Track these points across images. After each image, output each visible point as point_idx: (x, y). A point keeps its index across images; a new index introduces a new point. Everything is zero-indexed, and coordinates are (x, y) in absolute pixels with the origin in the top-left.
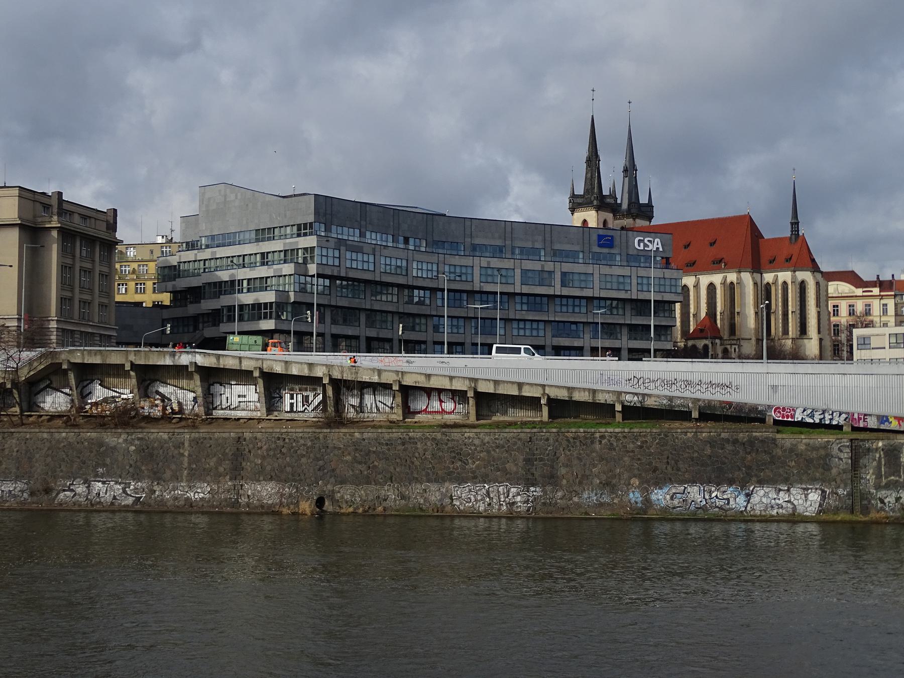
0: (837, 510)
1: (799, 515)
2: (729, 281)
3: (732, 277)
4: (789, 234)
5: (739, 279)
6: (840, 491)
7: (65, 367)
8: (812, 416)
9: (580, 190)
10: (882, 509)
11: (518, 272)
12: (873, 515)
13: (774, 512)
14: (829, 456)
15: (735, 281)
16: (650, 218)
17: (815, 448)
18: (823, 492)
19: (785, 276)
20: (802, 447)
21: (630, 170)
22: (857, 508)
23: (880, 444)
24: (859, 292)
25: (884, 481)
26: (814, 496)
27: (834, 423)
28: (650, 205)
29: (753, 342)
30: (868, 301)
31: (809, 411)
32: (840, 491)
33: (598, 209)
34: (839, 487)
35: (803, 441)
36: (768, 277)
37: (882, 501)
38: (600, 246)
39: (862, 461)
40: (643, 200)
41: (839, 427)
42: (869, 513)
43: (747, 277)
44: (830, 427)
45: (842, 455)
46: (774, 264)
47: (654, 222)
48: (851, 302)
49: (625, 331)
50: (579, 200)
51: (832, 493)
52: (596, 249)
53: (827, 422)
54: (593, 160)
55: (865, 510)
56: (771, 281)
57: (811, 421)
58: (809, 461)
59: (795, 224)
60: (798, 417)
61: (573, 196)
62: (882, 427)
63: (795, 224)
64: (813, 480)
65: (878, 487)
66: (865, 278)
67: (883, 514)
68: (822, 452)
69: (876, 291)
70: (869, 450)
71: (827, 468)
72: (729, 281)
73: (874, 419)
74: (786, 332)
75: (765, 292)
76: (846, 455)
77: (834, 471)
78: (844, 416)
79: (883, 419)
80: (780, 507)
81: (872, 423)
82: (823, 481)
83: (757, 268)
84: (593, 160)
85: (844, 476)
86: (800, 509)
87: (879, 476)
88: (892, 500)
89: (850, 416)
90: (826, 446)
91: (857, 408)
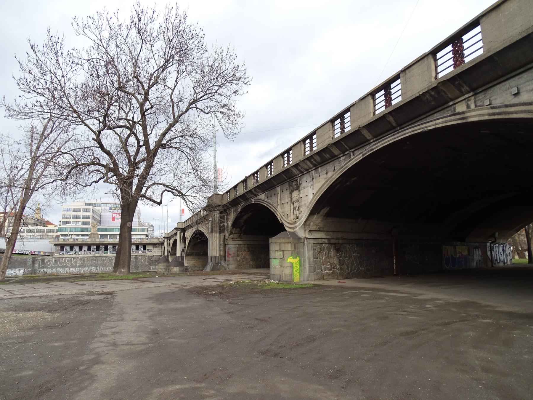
0: (28, 274)
1: (18, 276)
6: (29, 269)
8: (21, 252)
10: (39, 273)
12: (37, 275)
13: (11, 275)
14: (27, 261)
17: (23, 260)
18: (24, 270)
20: (19, 259)
22: (33, 273)
23: (40, 258)
25: (40, 267)
26: (22, 271)
27: (27, 253)
31: (20, 251)
32: (29, 269)
34: (28, 268)
35: (20, 257)
37: (40, 271)
39: (35, 262)
41: (27, 254)
42: (36, 274)
44: (25, 254)
45: (30, 261)
51: (27, 270)
53: (25, 253)
55: (35, 274)
57: (20, 253)
58: (21, 263)
60: (17, 252)
62: (39, 254)
64: (22, 267)
65: (39, 268)
67: (40, 274)
68: (25, 260)
70: (37, 259)
71: (26, 264)
73: (37, 252)
76: (31, 261)
77: (28, 265)
78: (29, 252)
79: (39, 252)
80: (12, 274)
81: (36, 253)
82: (25, 267)
85: (30, 266)
86: (18, 274)
87: (39, 265)
88: (42, 271)
89: (31, 252)
90: (26, 259)
91: (33, 250)
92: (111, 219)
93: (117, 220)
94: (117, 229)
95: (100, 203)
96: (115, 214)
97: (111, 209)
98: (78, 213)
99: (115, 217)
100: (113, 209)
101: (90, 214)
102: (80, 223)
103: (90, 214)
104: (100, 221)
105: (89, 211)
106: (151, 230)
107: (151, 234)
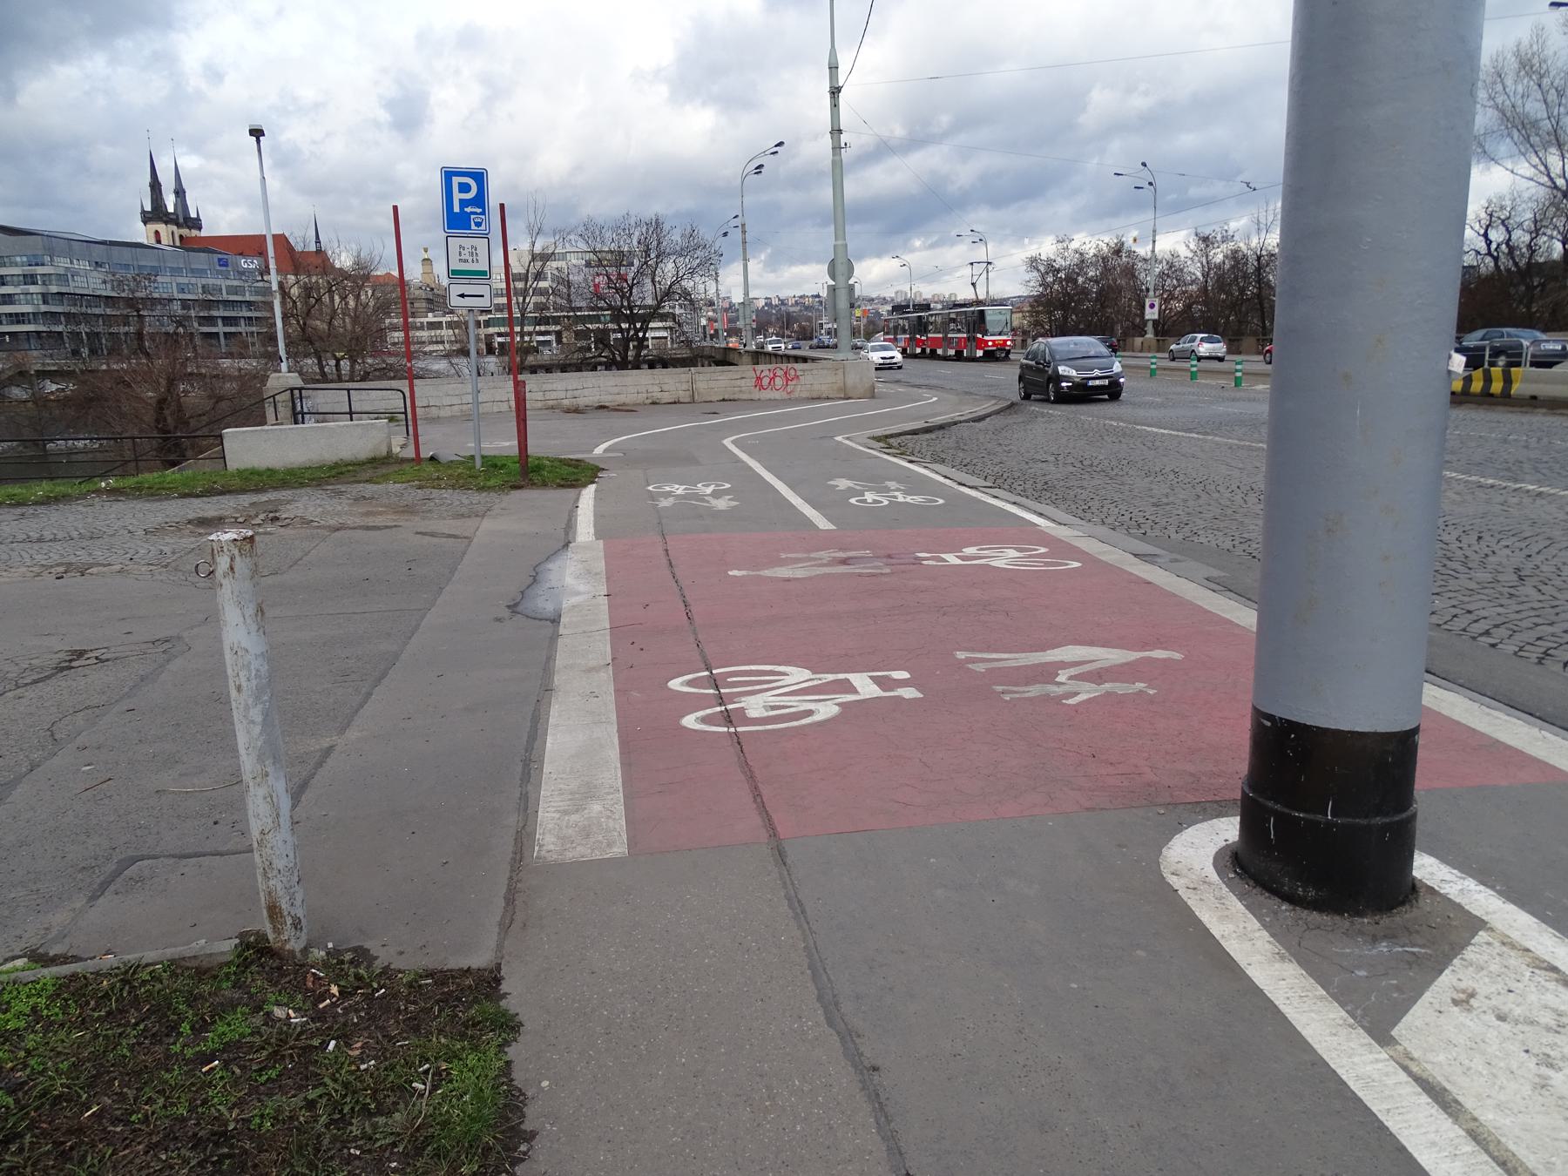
7: (32, 372)
9: (148, 208)
11: (174, 285)
16: (200, 228)
21: (180, 193)
28: (198, 219)
33: (166, 223)
38: (220, 265)
40: (193, 215)
47: (204, 233)
49: (242, 321)
50: (150, 216)
52: (218, 268)
54: (155, 186)
61: (143, 212)
63: (318, 241)
84: (155, 186)
95: (564, 251)
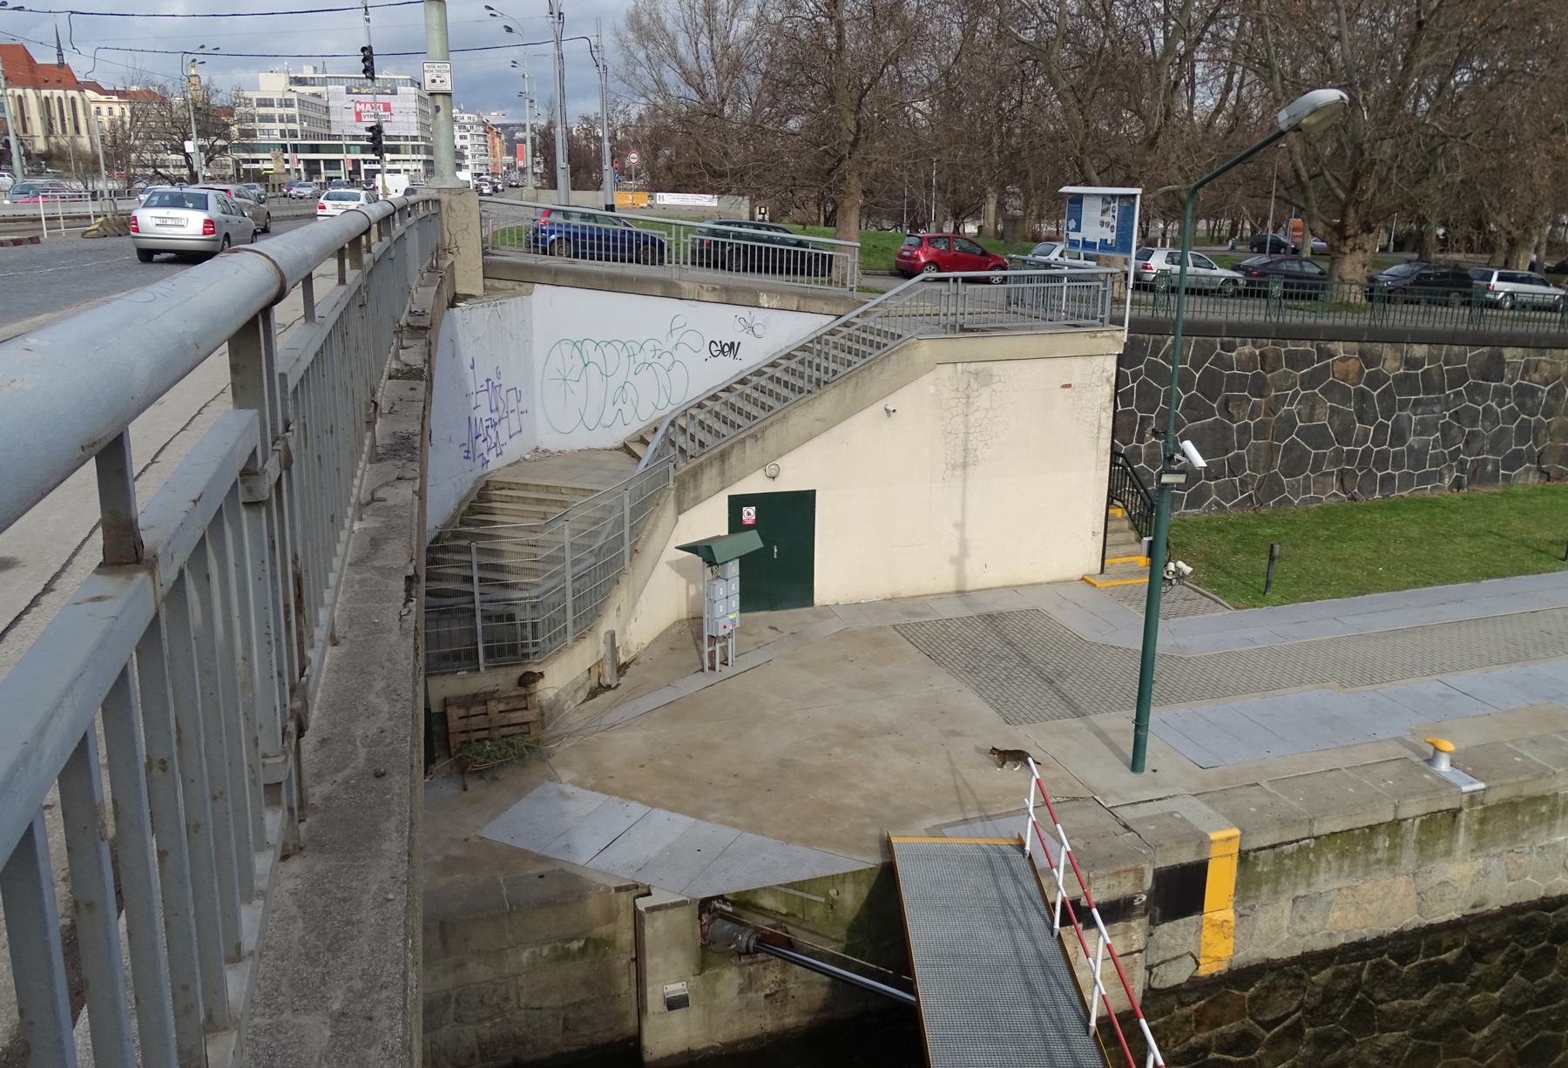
2: (16, 94)
3: (19, 91)
4: (56, 62)
5: (25, 93)
15: (22, 95)
19: (58, 93)
24: (103, 98)
29: (42, 138)
30: (110, 105)
36: (45, 93)
43: (30, 92)
46: (46, 84)
48: (98, 105)
56: (49, 96)
59: (60, 55)
63: (60, 55)
66: (106, 88)
69: (115, 98)
72: (16, 94)
74: (64, 131)
75: (46, 104)
83: (37, 87)
92: (354, 118)
93: (367, 119)
94: (358, 148)
95: (324, 76)
96: (360, 103)
97: (349, 92)
98: (269, 110)
99: (361, 111)
100: (355, 90)
101: (294, 111)
102: (277, 133)
103: (294, 111)
104: (329, 121)
105: (292, 106)
106: (479, 135)
107: (480, 145)
